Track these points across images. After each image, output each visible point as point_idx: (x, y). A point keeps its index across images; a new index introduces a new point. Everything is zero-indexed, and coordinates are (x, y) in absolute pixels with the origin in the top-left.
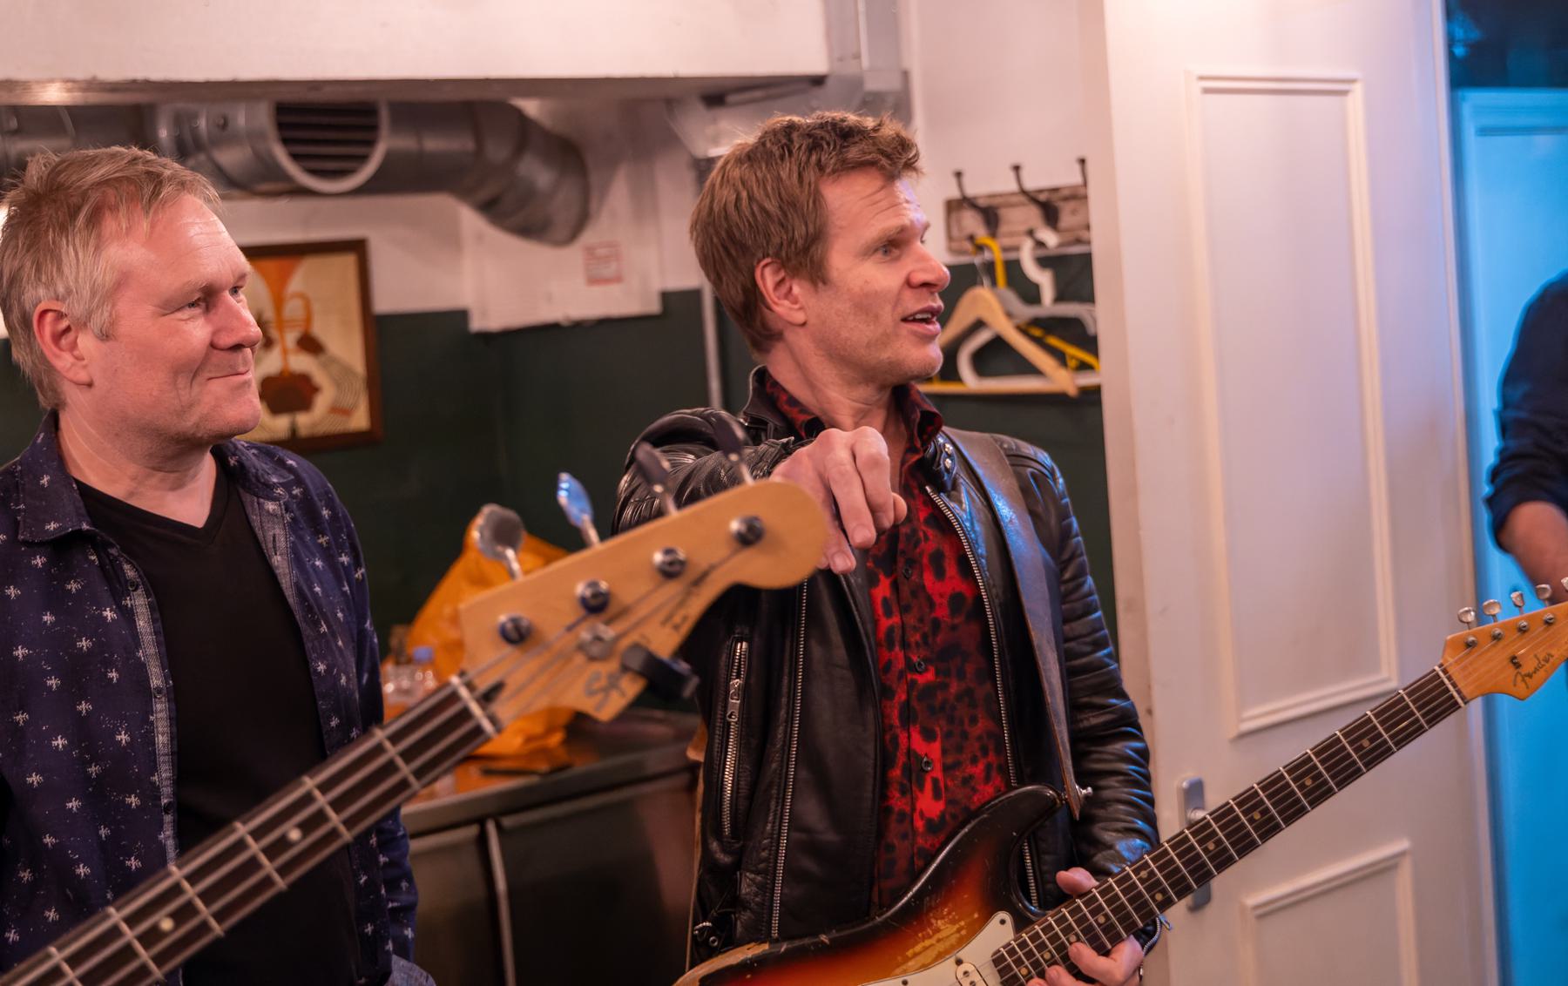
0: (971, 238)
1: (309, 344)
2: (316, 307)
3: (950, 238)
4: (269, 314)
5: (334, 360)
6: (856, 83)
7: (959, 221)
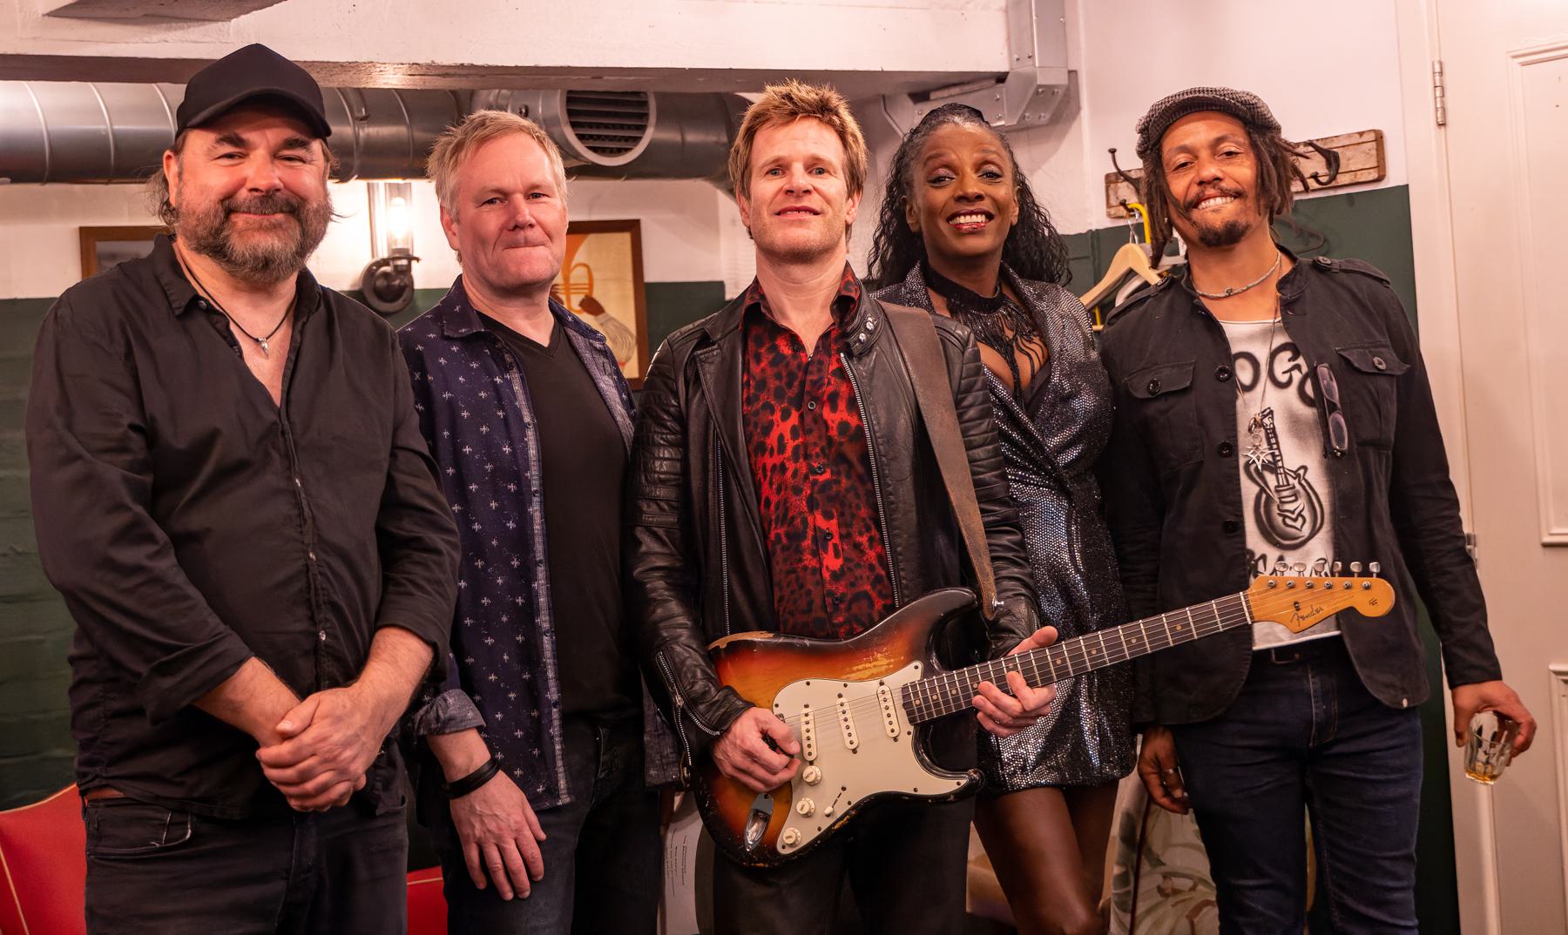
0: (1123, 204)
3: (1109, 205)
6: (1031, 78)
7: (1116, 193)
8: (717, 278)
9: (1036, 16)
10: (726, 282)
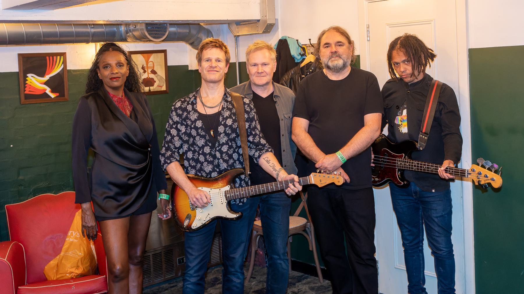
1: (153, 72)
2: (155, 64)
4: (145, 65)
5: (159, 75)
8: (187, 65)
9: (267, 6)
10: (189, 65)
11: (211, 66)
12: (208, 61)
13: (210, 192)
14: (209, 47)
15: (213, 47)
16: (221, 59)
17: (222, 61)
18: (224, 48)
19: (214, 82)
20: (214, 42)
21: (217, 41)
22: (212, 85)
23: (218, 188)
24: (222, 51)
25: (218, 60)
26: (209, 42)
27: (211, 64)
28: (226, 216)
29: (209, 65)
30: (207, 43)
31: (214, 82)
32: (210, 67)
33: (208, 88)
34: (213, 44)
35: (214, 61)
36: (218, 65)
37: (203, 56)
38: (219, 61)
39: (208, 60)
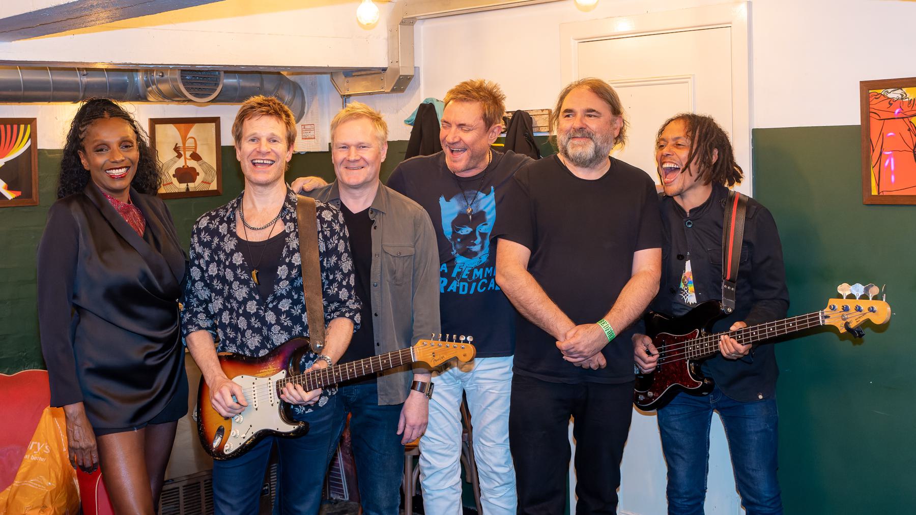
11: (258, 150)
12: (253, 140)
13: (254, 383)
14: (255, 115)
15: (263, 115)
16: (279, 137)
17: (280, 141)
18: (284, 117)
19: (266, 184)
20: (265, 106)
21: (271, 103)
22: (260, 188)
23: (265, 377)
24: (280, 122)
25: (272, 140)
26: (256, 105)
27: (260, 148)
28: (278, 429)
29: (256, 149)
30: (252, 107)
31: (266, 184)
32: (258, 152)
33: (255, 193)
34: (264, 109)
35: (264, 140)
36: (272, 150)
37: (244, 130)
38: (275, 141)
39: (255, 139)
